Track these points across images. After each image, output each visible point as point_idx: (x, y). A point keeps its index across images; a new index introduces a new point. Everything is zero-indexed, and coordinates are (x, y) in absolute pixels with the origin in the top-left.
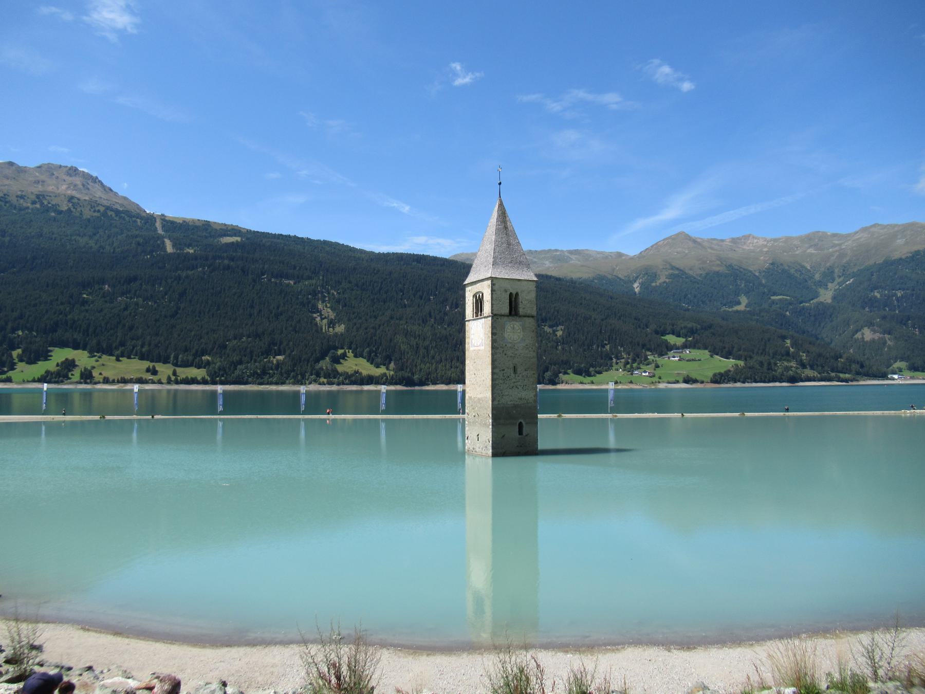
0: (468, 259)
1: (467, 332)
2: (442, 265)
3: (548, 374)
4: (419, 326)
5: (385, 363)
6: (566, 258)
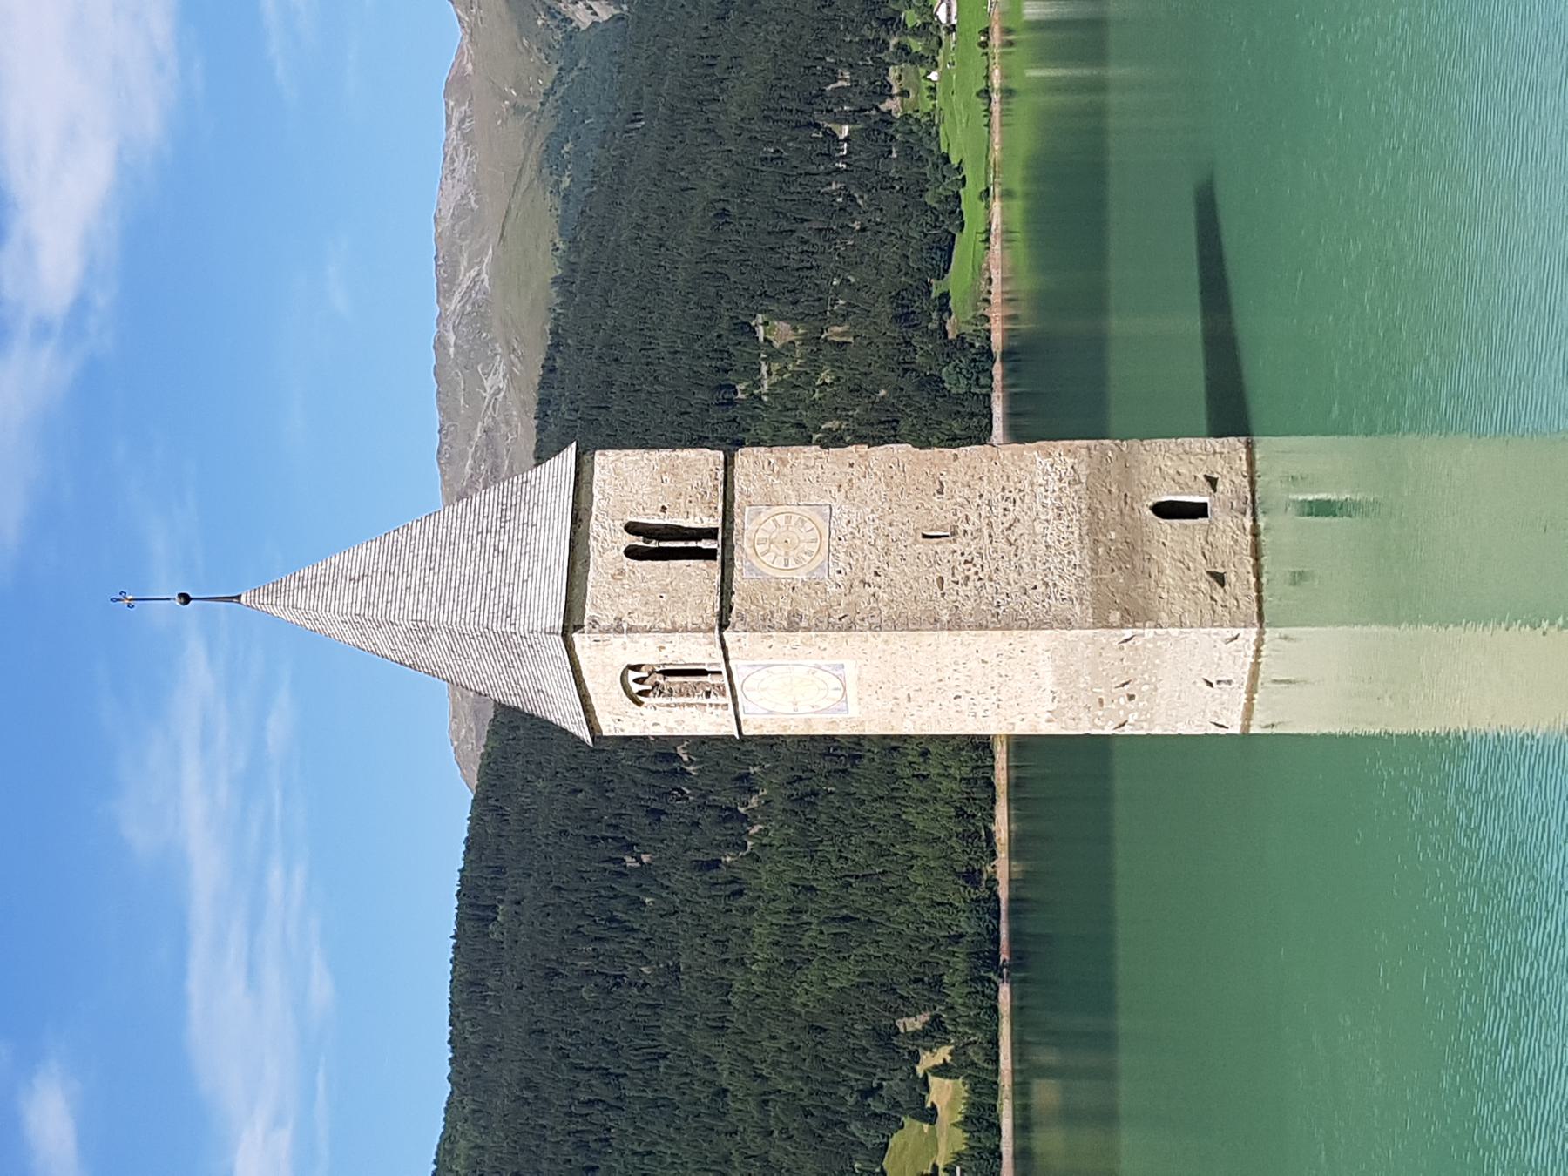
0: (476, 713)
2: (503, 818)
3: (955, 383)
4: (752, 910)
5: (910, 1052)
6: (469, 308)
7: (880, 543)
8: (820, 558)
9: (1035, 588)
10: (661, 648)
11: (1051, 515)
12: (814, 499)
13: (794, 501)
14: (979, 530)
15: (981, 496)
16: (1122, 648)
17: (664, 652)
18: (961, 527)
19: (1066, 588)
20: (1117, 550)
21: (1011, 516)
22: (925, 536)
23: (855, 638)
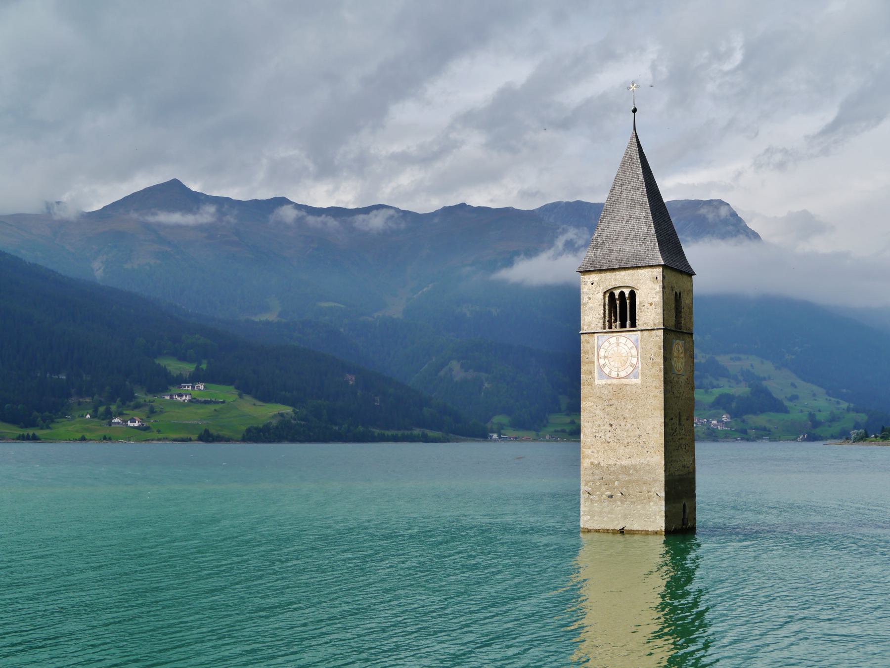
1: (587, 352)
10: (651, 304)
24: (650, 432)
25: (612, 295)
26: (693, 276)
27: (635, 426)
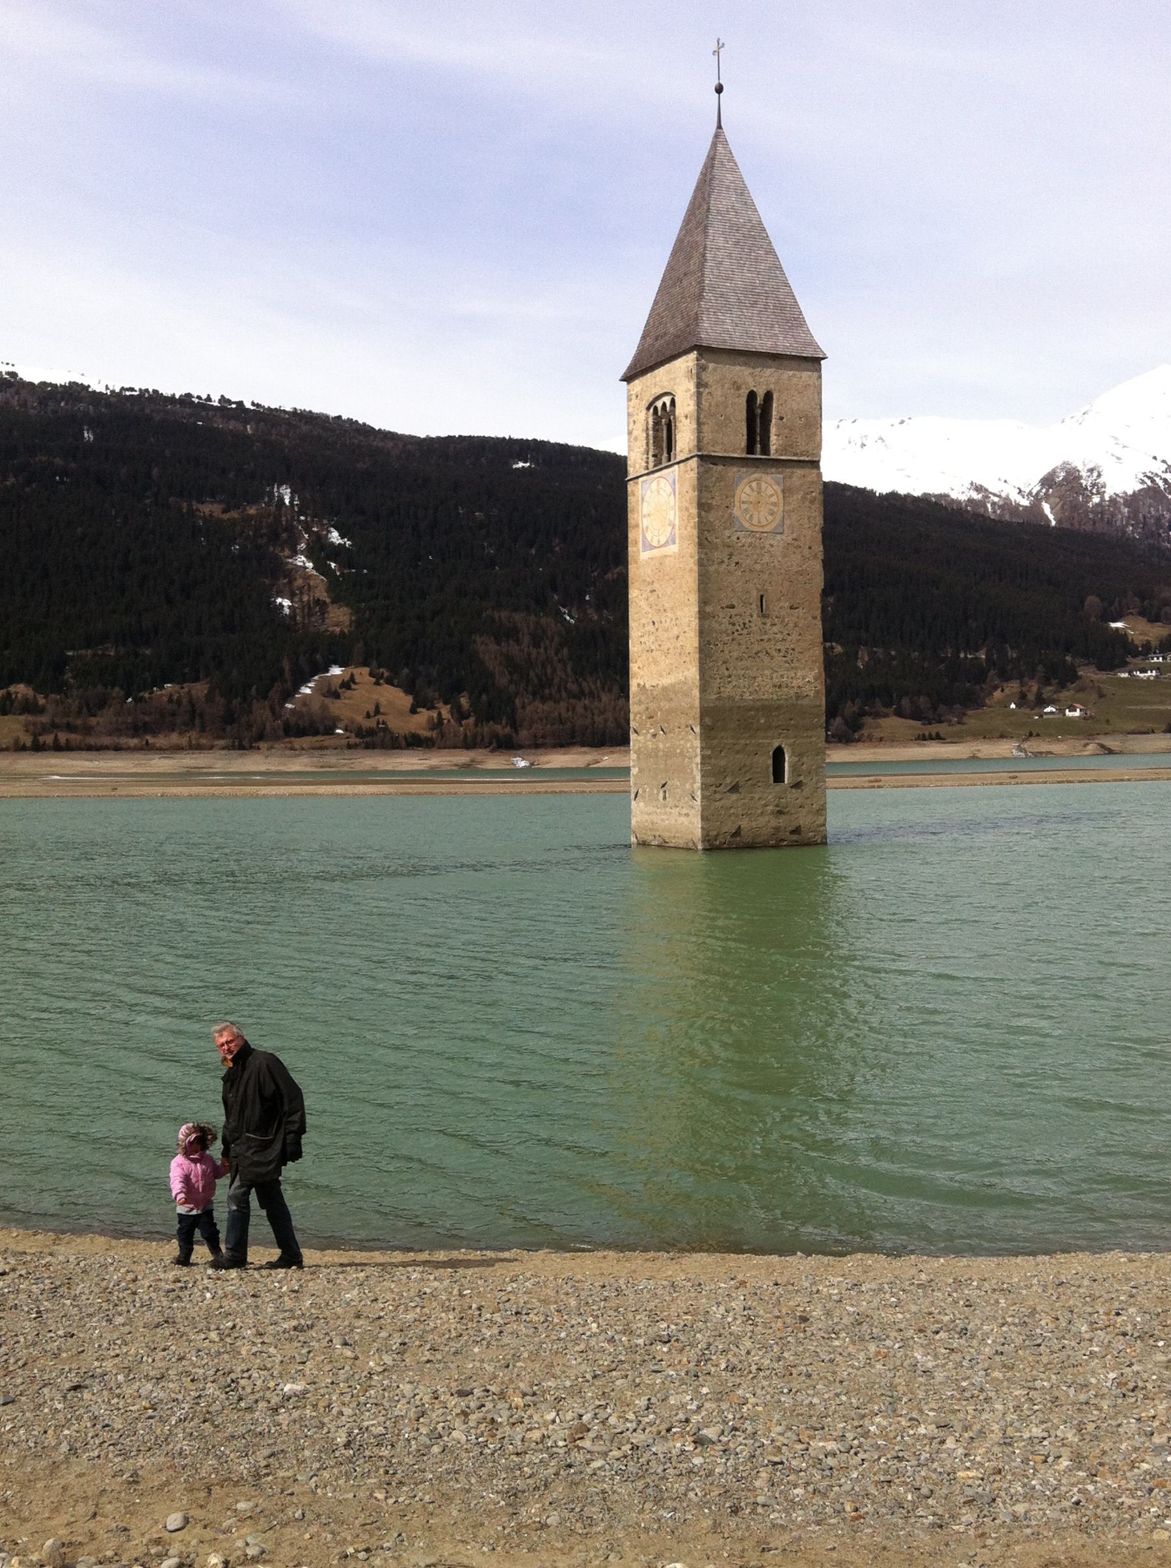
1: (633, 510)
7: (758, 567)
8: (747, 525)
9: (727, 669)
10: (686, 417)
11: (775, 680)
12: (787, 522)
13: (787, 508)
14: (766, 633)
15: (789, 634)
16: (687, 726)
17: (683, 419)
18: (769, 621)
19: (728, 690)
20: (752, 723)
21: (774, 653)
22: (762, 597)
23: (692, 549)
24: (687, 629)
25: (656, 409)
26: (822, 362)
27: (674, 622)
